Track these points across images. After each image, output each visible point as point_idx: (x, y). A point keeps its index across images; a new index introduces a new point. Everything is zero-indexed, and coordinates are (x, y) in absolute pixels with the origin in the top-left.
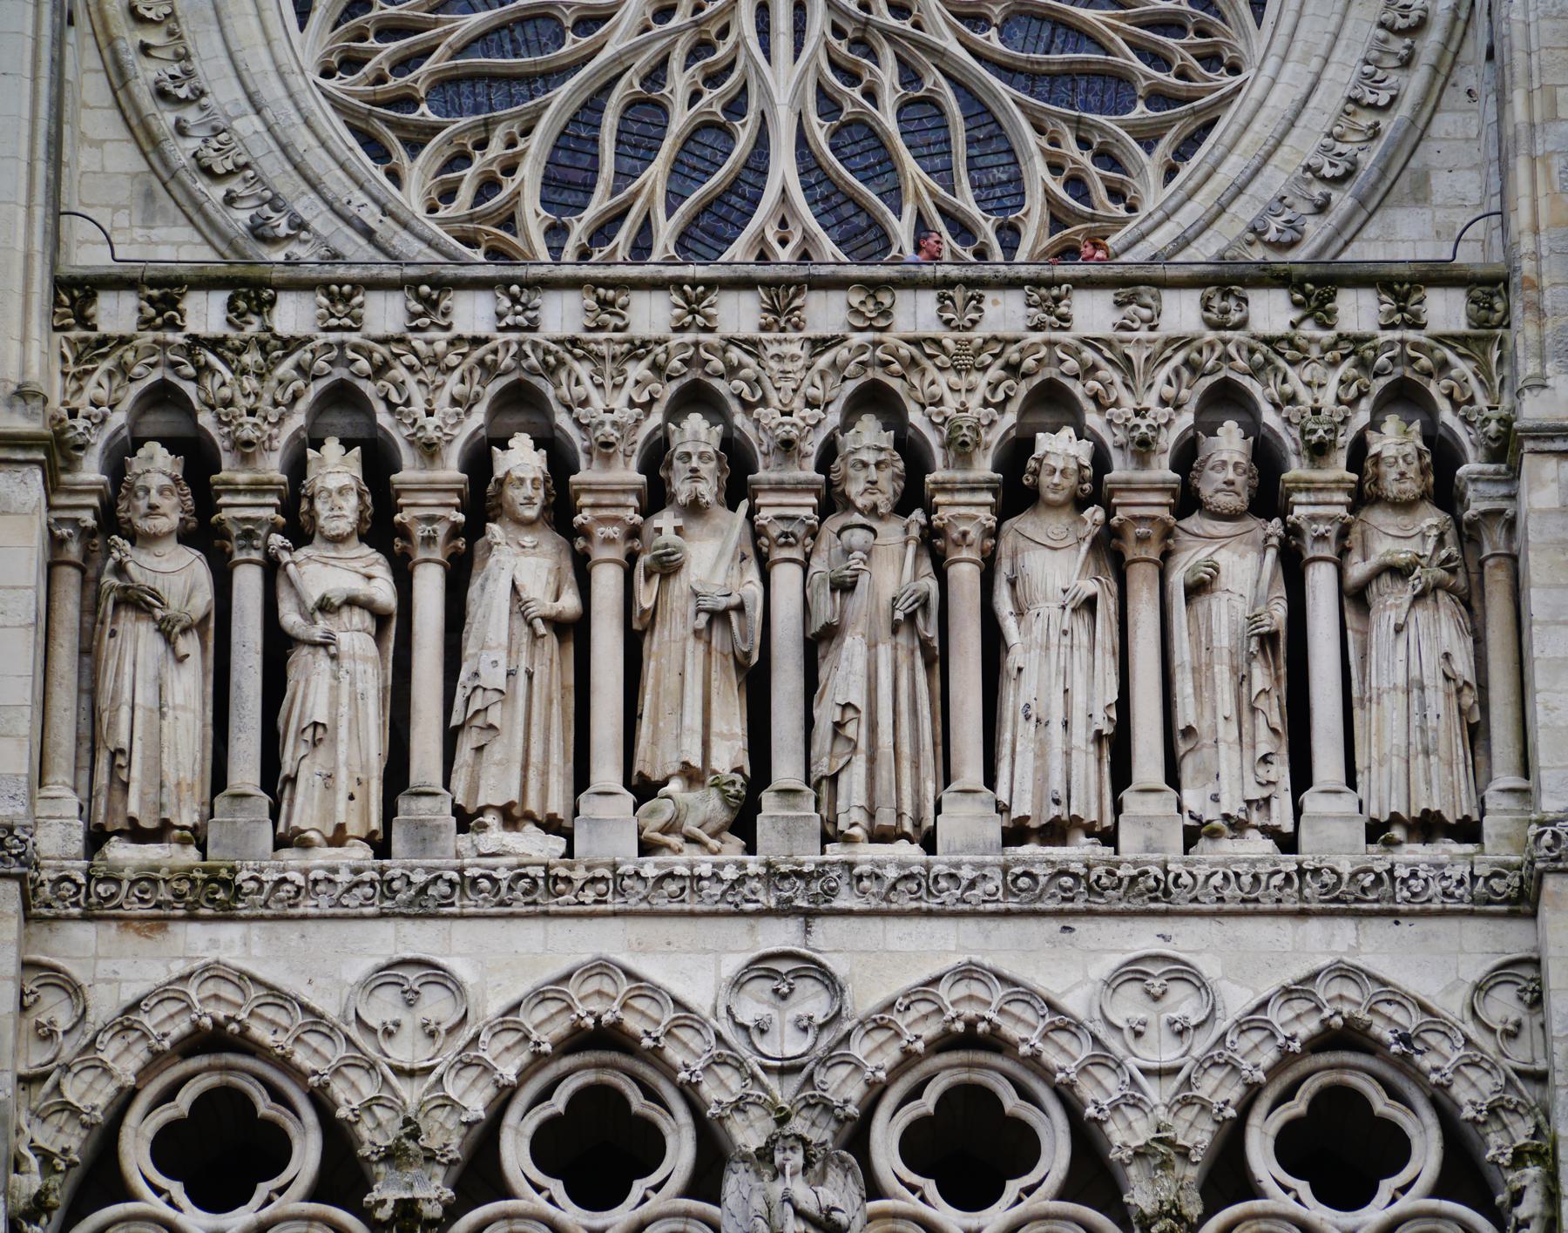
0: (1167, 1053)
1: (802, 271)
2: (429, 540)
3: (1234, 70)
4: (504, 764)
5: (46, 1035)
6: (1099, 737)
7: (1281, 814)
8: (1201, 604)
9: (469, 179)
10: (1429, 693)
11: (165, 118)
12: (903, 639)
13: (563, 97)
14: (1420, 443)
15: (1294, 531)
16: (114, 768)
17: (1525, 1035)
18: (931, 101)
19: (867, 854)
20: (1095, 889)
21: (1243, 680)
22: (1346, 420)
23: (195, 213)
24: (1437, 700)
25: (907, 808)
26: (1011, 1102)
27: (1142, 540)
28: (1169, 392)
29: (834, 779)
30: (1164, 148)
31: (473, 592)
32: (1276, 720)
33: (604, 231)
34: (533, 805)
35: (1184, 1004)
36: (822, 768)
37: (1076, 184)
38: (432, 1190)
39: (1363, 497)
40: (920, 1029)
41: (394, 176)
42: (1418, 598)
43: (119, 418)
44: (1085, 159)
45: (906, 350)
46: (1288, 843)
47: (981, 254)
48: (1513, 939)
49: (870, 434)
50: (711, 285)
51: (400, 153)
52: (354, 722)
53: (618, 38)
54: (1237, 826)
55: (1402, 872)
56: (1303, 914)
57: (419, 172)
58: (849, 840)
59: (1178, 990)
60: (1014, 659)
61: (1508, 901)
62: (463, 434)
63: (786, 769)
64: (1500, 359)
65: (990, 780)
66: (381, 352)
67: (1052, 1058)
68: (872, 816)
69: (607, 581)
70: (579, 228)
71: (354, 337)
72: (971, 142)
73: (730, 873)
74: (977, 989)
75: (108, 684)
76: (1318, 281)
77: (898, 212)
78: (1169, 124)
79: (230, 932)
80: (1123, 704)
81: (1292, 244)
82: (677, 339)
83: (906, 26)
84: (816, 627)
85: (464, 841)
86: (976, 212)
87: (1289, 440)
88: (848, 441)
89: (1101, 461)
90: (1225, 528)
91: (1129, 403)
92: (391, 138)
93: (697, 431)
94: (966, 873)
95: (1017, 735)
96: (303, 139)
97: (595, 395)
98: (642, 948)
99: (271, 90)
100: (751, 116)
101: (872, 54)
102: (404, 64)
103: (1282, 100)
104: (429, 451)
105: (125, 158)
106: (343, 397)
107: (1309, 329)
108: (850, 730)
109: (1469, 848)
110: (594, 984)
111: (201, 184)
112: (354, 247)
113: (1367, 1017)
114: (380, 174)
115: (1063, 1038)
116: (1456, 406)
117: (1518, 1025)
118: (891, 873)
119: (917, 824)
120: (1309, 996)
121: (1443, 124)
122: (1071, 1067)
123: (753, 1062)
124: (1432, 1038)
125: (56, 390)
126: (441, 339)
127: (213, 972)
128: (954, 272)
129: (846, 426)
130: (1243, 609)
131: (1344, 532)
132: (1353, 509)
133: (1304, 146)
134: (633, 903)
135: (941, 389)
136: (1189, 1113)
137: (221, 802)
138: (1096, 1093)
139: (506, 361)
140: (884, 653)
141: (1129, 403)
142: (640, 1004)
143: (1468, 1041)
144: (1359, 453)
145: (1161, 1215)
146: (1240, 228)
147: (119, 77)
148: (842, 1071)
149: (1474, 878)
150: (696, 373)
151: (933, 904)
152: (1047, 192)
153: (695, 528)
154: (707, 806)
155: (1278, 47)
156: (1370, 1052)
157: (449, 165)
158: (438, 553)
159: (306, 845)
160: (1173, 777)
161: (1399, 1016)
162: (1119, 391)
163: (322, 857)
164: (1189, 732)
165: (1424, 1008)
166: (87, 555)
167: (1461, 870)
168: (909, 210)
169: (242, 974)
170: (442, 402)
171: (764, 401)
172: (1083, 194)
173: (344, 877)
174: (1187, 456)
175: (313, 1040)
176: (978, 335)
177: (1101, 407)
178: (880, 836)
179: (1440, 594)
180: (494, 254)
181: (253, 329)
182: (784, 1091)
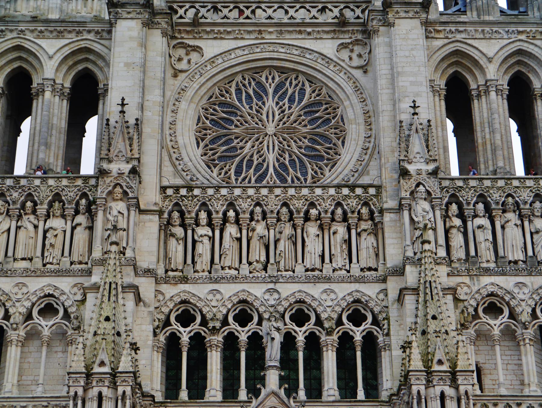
0: (330, 304)
1: (274, 185)
2: (217, 226)
3: (340, 155)
4: (229, 260)
5: (159, 301)
6: (320, 255)
7: (347, 267)
8: (335, 235)
9: (223, 172)
11: (177, 163)
12: (290, 241)
13: (237, 159)
15: (349, 224)
16: (169, 261)
18: (294, 160)
19: (284, 273)
20: (319, 279)
21: (341, 247)
23: (182, 177)
24: (371, 250)
25: (290, 266)
26: (306, 311)
27: (326, 226)
28: (330, 203)
29: (279, 262)
30: (329, 167)
31: (224, 234)
32: (347, 253)
33: (244, 180)
34: (233, 266)
35: (333, 296)
36: (277, 260)
37: (316, 172)
38: (218, 325)
39: (360, 219)
40: (292, 300)
41: (212, 171)
42: (368, 234)
43: (170, 208)
44: (317, 168)
45: (290, 197)
46: (348, 272)
47: (301, 183)
48: (383, 286)
49: (284, 210)
50: (260, 187)
51: (213, 168)
52: (206, 254)
53: (246, 150)
54: (341, 269)
55: (366, 276)
56: (351, 282)
57: (216, 171)
58: (281, 271)
59: (332, 294)
60: (307, 244)
62: (222, 210)
63: (272, 260)
65: (303, 262)
66: (210, 197)
67: (312, 304)
68: (285, 268)
69: (244, 232)
70: (240, 179)
71: (206, 195)
72: (300, 166)
73: (263, 276)
74: (301, 294)
75: (168, 248)
76: (353, 186)
77: (289, 176)
78: (330, 163)
79: (187, 285)
80: (323, 251)
81: (349, 181)
82: (255, 195)
83: (290, 149)
84: (276, 239)
85: (223, 271)
86: (300, 176)
87: (348, 210)
88: (281, 211)
89: (320, 214)
90: (339, 224)
91: (324, 205)
92: (211, 166)
93: (258, 209)
94: (299, 276)
95: (307, 255)
96: (198, 166)
97: (243, 204)
98: (250, 288)
99: (193, 158)
100: (266, 162)
101: (285, 153)
102: (214, 154)
103: (347, 160)
104: (217, 212)
105: (171, 169)
106: (204, 204)
107: (351, 194)
108: (282, 255)
110: (243, 293)
111: (183, 173)
112: (206, 182)
113: (360, 298)
114: (210, 171)
115: (314, 301)
116: (374, 205)
118: (288, 276)
119: (292, 269)
120: (352, 295)
121: (371, 163)
122: (316, 306)
123: (267, 305)
124: (371, 301)
125: (161, 203)
126: (219, 195)
127: (184, 291)
128: (297, 185)
129: (281, 208)
130: (341, 236)
131: (357, 224)
132: (358, 221)
133: (350, 166)
134: (248, 281)
135: (295, 203)
136: (334, 313)
137: (185, 266)
138: (319, 310)
139: (229, 199)
140: (287, 243)
141: (324, 205)
142: (249, 296)
144: (359, 212)
145: (329, 328)
146: (341, 179)
147: (170, 157)
148: (281, 306)
150: (258, 201)
151: (294, 281)
152: (312, 174)
153: (258, 224)
154: (260, 266)
155: (346, 152)
157: (220, 170)
158: (219, 228)
159: (198, 272)
160: (331, 262)
161: (365, 298)
162: (322, 203)
163: (201, 274)
164: (333, 255)
165: (369, 297)
166: (165, 228)
167: (375, 276)
168: (290, 176)
169: (189, 292)
170: (219, 205)
171: (268, 205)
172: (317, 174)
173: (204, 277)
174: (333, 213)
175: (200, 302)
176: (301, 195)
177: (320, 205)
178: (286, 271)
180: (227, 183)
181: (190, 194)
182: (271, 310)
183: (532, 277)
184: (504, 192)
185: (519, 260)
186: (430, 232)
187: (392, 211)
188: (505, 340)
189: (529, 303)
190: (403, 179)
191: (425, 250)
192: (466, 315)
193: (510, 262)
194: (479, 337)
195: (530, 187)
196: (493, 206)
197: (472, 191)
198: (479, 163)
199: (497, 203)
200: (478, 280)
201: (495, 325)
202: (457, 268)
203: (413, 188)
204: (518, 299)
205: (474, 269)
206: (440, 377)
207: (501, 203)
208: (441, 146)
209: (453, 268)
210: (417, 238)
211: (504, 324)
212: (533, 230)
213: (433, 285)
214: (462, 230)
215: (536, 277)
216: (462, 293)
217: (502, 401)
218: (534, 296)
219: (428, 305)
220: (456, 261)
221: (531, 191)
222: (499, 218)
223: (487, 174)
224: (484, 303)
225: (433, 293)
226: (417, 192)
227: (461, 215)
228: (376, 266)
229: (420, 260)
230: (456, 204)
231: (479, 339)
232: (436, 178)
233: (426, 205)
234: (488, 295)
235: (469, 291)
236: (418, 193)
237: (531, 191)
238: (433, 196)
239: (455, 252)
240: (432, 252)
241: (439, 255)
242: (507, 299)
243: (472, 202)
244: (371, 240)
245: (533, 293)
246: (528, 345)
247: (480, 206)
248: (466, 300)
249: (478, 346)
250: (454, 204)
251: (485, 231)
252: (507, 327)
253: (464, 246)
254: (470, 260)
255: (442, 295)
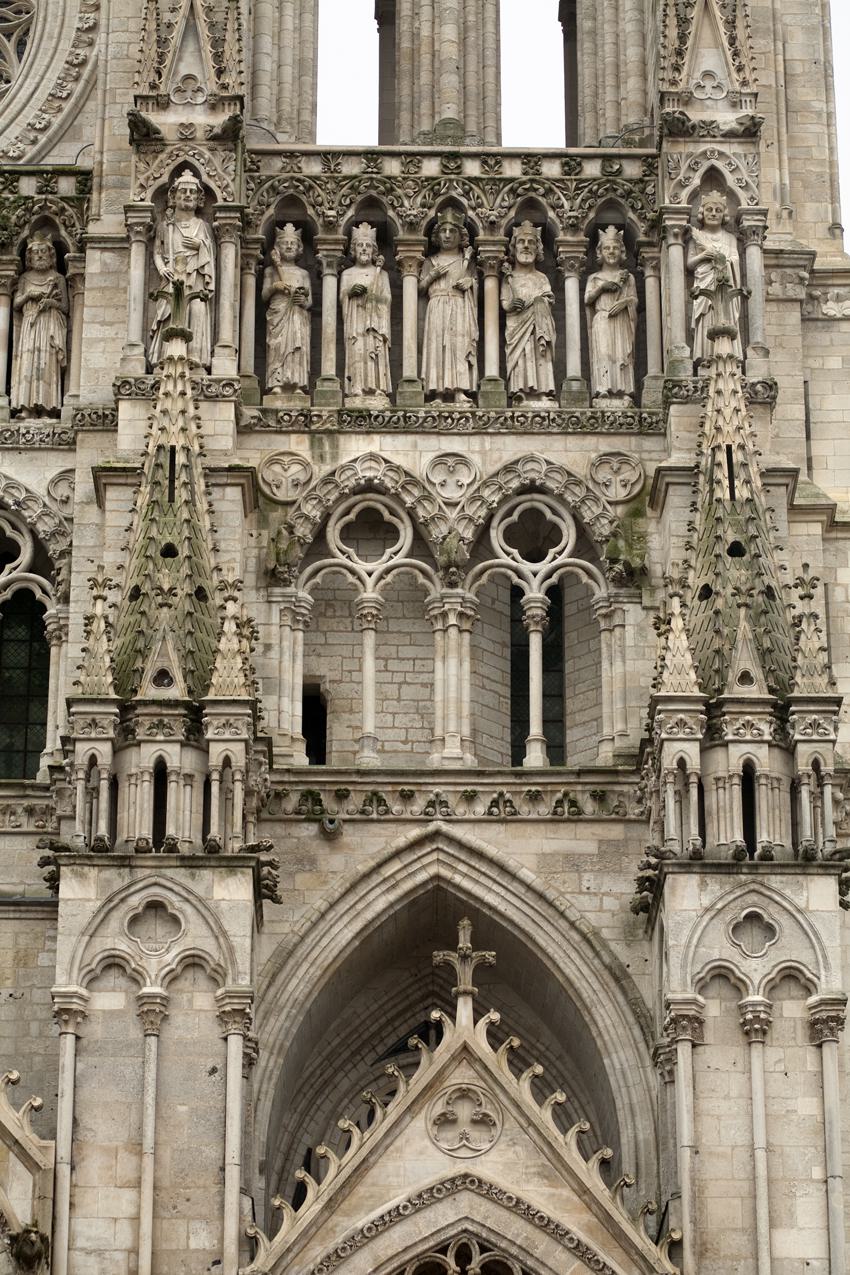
10: (43, 354)
14: (50, 244)
17: (71, 502)
22: (18, 234)
24: (45, 357)
42: (41, 312)
55: (23, 431)
61: (68, 444)
64: (88, 208)
76: (11, 172)
109: (54, 421)
116: (66, 227)
117: (68, 498)
124: (30, 503)
143: (45, 505)
149: (54, 434)
156: (5, 509)
165: (27, 490)
179: (54, 312)
183: (487, 439)
184: (437, 195)
185: (459, 390)
186: (199, 306)
187: (109, 245)
188: (404, 617)
189: (469, 511)
190: (138, 152)
191: (171, 359)
192: (283, 545)
193: (431, 396)
194: (332, 606)
195: (512, 180)
196: (402, 235)
197: (345, 191)
198: (399, 110)
199: (412, 226)
200: (335, 446)
201: (370, 574)
202: (277, 411)
203: (165, 179)
204: (439, 500)
205: (325, 414)
206: (155, 720)
207: (424, 223)
208: (288, 57)
209: (264, 411)
210: (159, 322)
211: (395, 572)
212: (506, 305)
213: (180, 459)
214: (309, 301)
215: (499, 440)
216: (283, 481)
217: (359, 788)
218: (486, 493)
219: (156, 514)
220: (277, 390)
221: (513, 191)
222: (414, 270)
223: (413, 142)
224: (347, 512)
225: (177, 483)
226: (175, 191)
227: (306, 258)
228: (54, 403)
229: (156, 386)
230: (297, 226)
231: (330, 613)
232: (235, 150)
233: (195, 229)
234: (359, 490)
235: (303, 478)
236: (178, 194)
237: (513, 191)
238: (220, 202)
239: (278, 365)
240: (193, 366)
241: (217, 373)
242: (409, 500)
243: (343, 221)
244: (52, 327)
245: (485, 484)
246: (453, 632)
247: (365, 235)
248: (294, 502)
249: (325, 633)
250: (289, 228)
251: (369, 305)
252: (406, 575)
253: (306, 349)
254: (321, 386)
255: (203, 487)
